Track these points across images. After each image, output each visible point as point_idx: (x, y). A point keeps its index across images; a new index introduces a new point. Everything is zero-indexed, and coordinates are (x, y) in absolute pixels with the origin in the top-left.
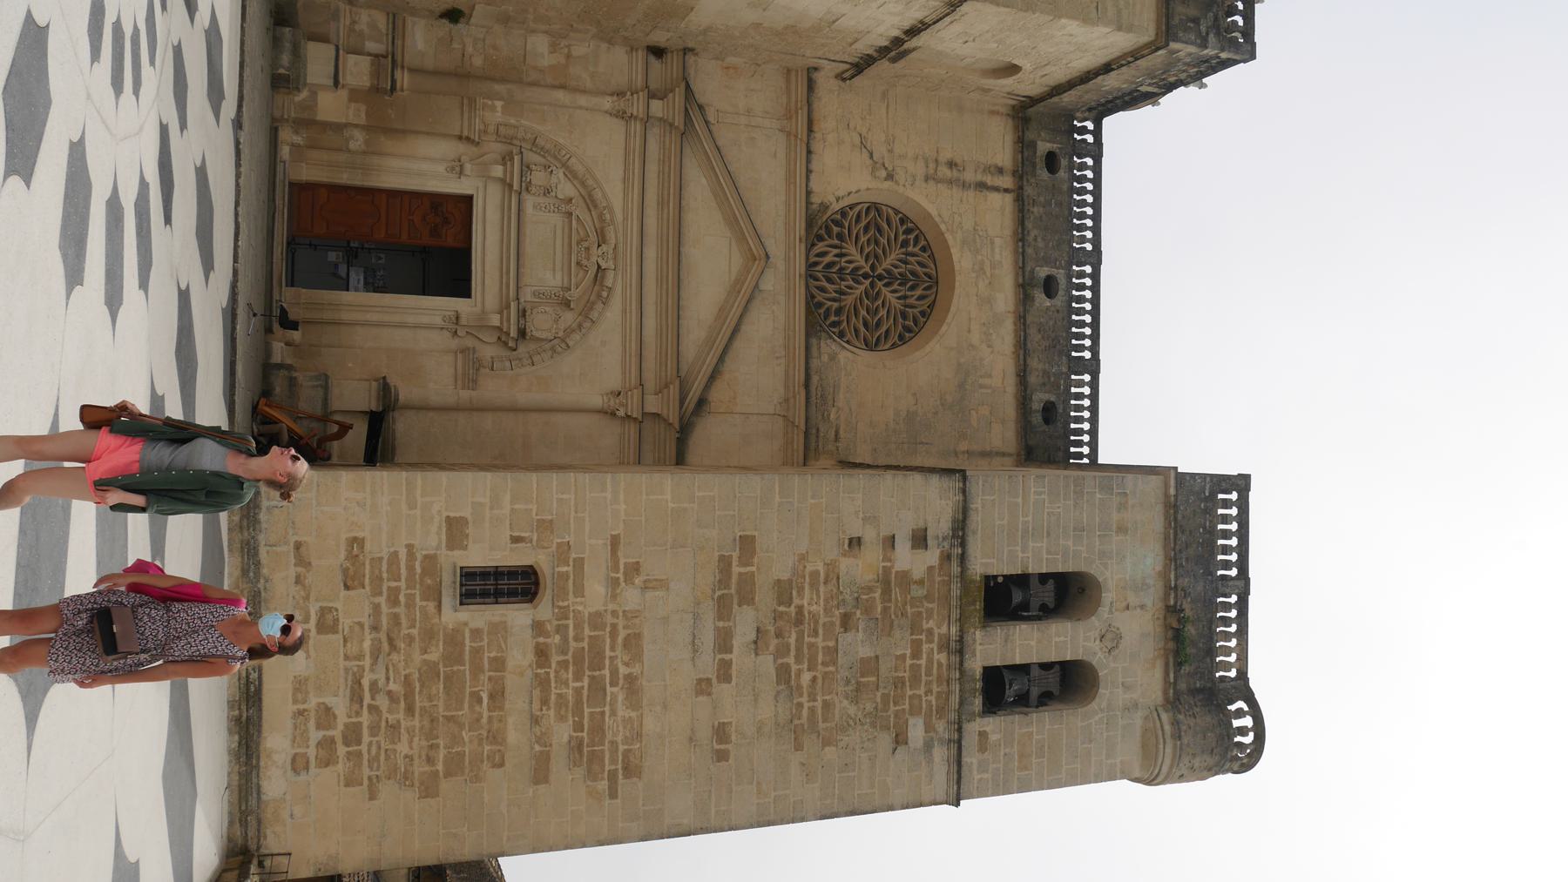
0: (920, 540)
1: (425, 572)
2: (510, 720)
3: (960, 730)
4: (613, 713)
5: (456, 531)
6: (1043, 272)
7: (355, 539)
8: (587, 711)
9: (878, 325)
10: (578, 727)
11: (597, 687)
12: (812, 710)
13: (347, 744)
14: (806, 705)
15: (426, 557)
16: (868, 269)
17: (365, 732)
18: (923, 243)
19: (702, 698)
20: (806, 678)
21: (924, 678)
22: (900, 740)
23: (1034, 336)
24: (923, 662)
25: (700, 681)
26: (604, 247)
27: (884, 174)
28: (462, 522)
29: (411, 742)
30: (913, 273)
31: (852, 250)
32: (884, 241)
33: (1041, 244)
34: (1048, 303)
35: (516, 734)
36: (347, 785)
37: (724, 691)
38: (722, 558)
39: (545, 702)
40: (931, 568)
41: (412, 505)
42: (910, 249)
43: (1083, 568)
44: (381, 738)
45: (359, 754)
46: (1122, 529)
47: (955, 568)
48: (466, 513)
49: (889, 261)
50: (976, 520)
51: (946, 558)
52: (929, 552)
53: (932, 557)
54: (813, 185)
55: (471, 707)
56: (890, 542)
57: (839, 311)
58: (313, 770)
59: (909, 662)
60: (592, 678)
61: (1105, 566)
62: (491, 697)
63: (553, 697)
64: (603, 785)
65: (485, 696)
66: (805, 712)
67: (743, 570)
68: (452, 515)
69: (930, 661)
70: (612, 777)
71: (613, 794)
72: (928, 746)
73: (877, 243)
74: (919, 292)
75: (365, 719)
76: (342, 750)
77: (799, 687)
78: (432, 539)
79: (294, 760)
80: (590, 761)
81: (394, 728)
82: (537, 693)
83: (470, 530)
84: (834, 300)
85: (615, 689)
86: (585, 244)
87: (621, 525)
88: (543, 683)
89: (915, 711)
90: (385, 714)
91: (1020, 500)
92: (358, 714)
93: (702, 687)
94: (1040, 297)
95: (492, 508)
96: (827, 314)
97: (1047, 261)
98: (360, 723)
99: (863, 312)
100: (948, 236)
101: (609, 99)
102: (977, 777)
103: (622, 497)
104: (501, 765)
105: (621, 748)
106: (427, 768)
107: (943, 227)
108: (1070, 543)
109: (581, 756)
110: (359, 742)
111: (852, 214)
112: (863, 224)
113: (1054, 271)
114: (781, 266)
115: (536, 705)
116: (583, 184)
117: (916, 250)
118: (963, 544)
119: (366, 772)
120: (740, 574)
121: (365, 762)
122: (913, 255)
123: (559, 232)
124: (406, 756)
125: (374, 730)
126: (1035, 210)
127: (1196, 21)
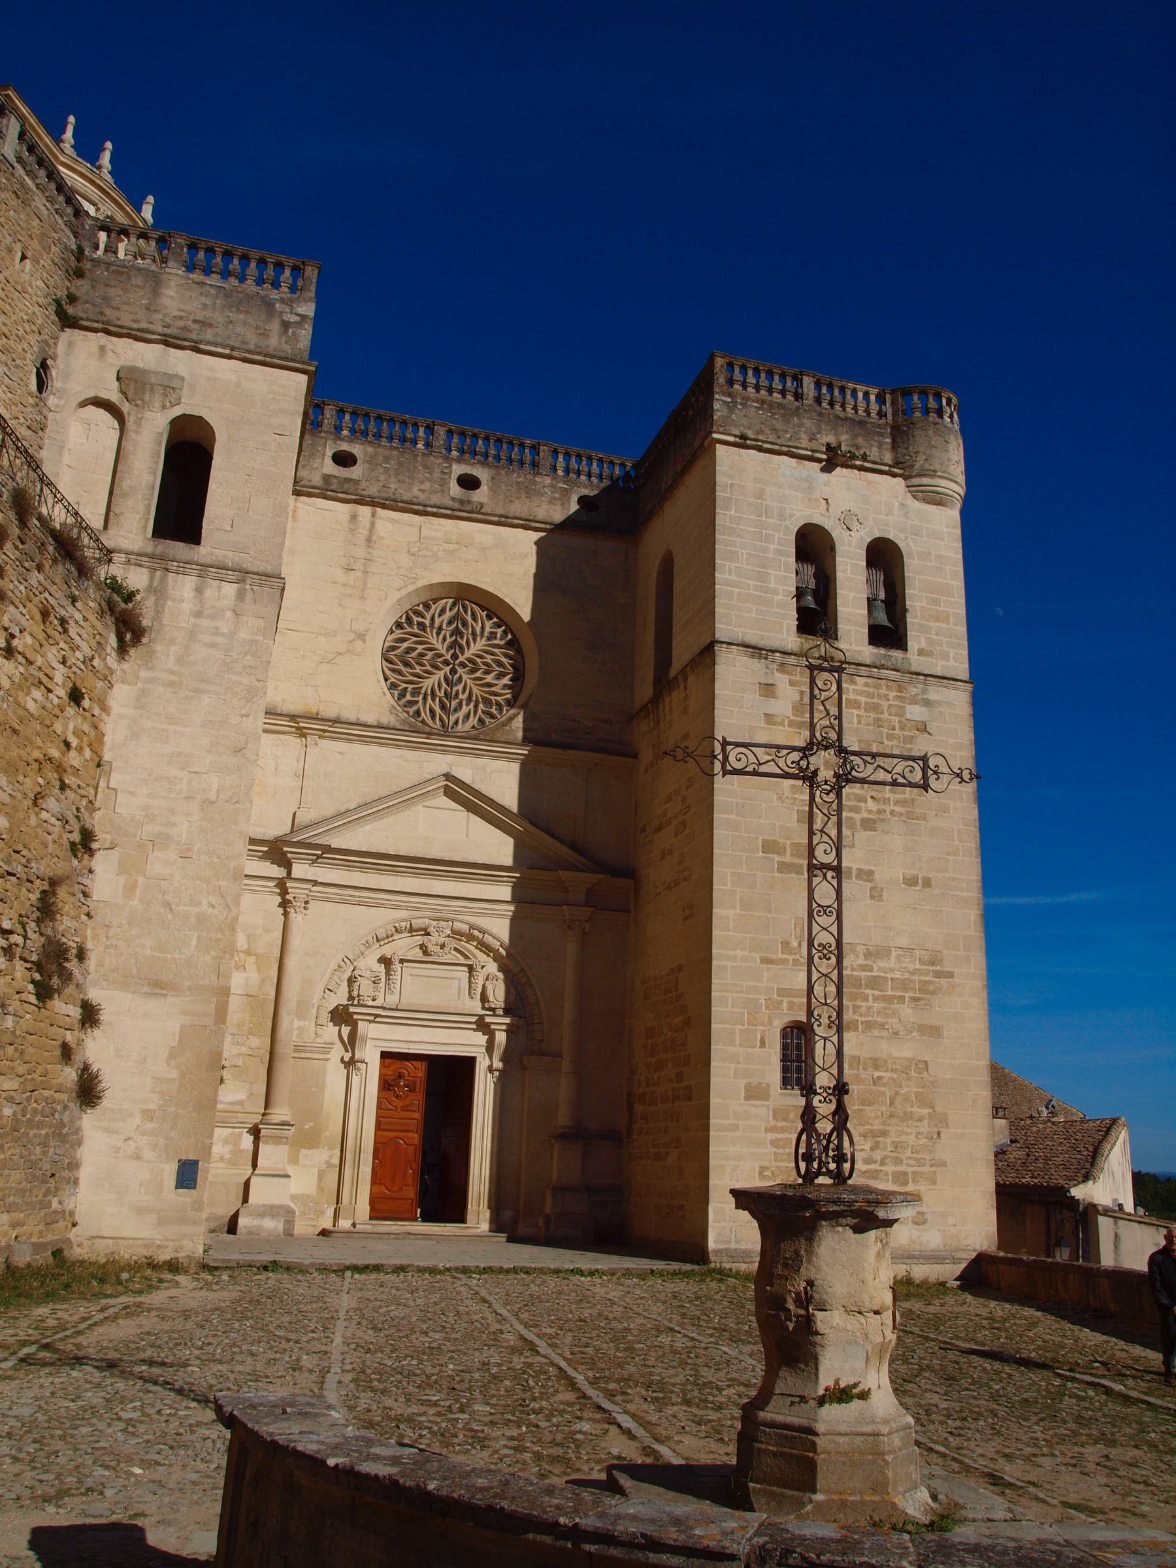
0: (768, 689)
1: (785, 1119)
2: (895, 1054)
3: (917, 674)
4: (892, 970)
5: (755, 1093)
6: (455, 490)
7: (760, 1173)
8: (890, 993)
9: (500, 664)
10: (902, 999)
11: (875, 982)
12: (897, 803)
13: (907, 1183)
14: (892, 807)
15: (774, 1117)
16: (447, 669)
17: (899, 1168)
18: (421, 608)
19: (884, 897)
20: (871, 804)
21: (875, 700)
22: (923, 728)
23: (518, 508)
24: (863, 700)
25: (872, 897)
26: (431, 930)
27: (359, 643)
28: (748, 1087)
29: (907, 1134)
30: (450, 623)
31: (427, 684)
32: (420, 648)
33: (427, 486)
34: (484, 488)
35: (905, 1050)
36: (935, 1183)
37: (881, 875)
38: (780, 870)
39: (882, 1026)
40: (791, 683)
41: (736, 1128)
42: (427, 622)
43: (792, 538)
44: (903, 1157)
45: (914, 1173)
46: (760, 495)
47: (792, 660)
48: (742, 1083)
49: (439, 646)
50: (753, 637)
51: (782, 667)
52: (778, 684)
53: (782, 680)
54: (370, 719)
55: (884, 1085)
56: (769, 718)
57: (487, 702)
58: (924, 1209)
59: (862, 712)
60: (867, 986)
61: (791, 516)
62: (877, 1068)
63: (879, 1019)
64: (944, 982)
65: (877, 1074)
66: (898, 809)
67: (788, 853)
68: (743, 1095)
69: (861, 693)
70: (938, 975)
71: (951, 975)
72: (927, 703)
73: (422, 655)
74: (469, 618)
75: (890, 1168)
76: (910, 1188)
77: (879, 812)
78: (761, 1111)
79: (916, 1223)
80: (927, 992)
81: (896, 1146)
82: (876, 1032)
83: (755, 1081)
84: (476, 707)
85: (875, 968)
86: (431, 948)
87: (753, 954)
88: (869, 1026)
89: (901, 713)
90: (887, 1153)
91: (736, 590)
92: (886, 1174)
93: (876, 894)
94: (481, 495)
95: (738, 1063)
96: (492, 716)
97: (444, 483)
98: (893, 1172)
99: (489, 678)
100: (421, 583)
101: (292, 915)
102: (952, 662)
103: (731, 953)
104: (926, 1063)
105: (918, 966)
106: (926, 1121)
107: (411, 588)
108: (772, 547)
109: (922, 999)
110: (906, 1173)
111: (393, 678)
112: (401, 667)
113: (454, 477)
114: (450, 758)
115: (885, 1034)
116: (368, 945)
117: (429, 617)
118: (773, 651)
119: (926, 1169)
120: (792, 855)
121: (920, 1169)
122: (433, 619)
123: (415, 972)
124: (917, 1137)
125: (897, 1161)
126: (393, 486)
127: (286, 325)
